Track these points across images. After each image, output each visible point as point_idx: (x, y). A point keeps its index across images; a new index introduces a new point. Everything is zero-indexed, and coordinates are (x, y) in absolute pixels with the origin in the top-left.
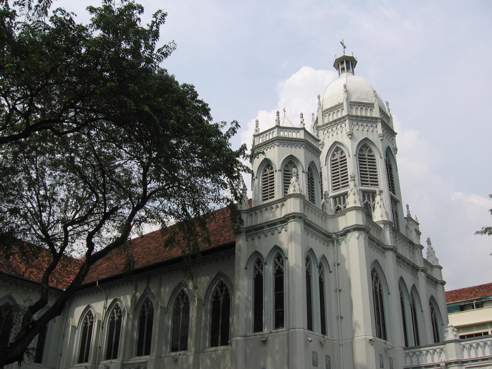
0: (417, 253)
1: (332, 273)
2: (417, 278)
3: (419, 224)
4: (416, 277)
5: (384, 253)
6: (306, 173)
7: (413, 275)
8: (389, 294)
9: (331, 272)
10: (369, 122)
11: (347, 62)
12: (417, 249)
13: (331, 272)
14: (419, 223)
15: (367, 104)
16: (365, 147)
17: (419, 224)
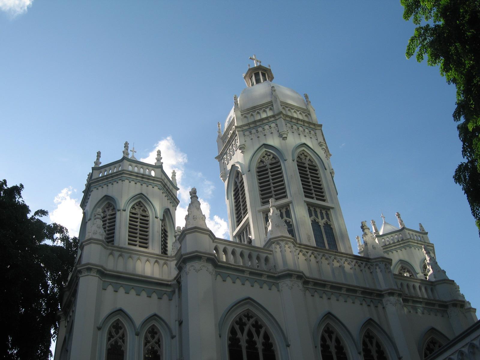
0: (378, 270)
1: (174, 339)
2: (384, 308)
3: (427, 233)
4: (380, 307)
5: (277, 285)
6: (119, 210)
7: (369, 306)
8: (288, 346)
9: (173, 337)
10: (266, 124)
11: (257, 75)
12: (377, 265)
13: (173, 337)
14: (426, 232)
15: (263, 106)
16: (266, 157)
17: (427, 233)
